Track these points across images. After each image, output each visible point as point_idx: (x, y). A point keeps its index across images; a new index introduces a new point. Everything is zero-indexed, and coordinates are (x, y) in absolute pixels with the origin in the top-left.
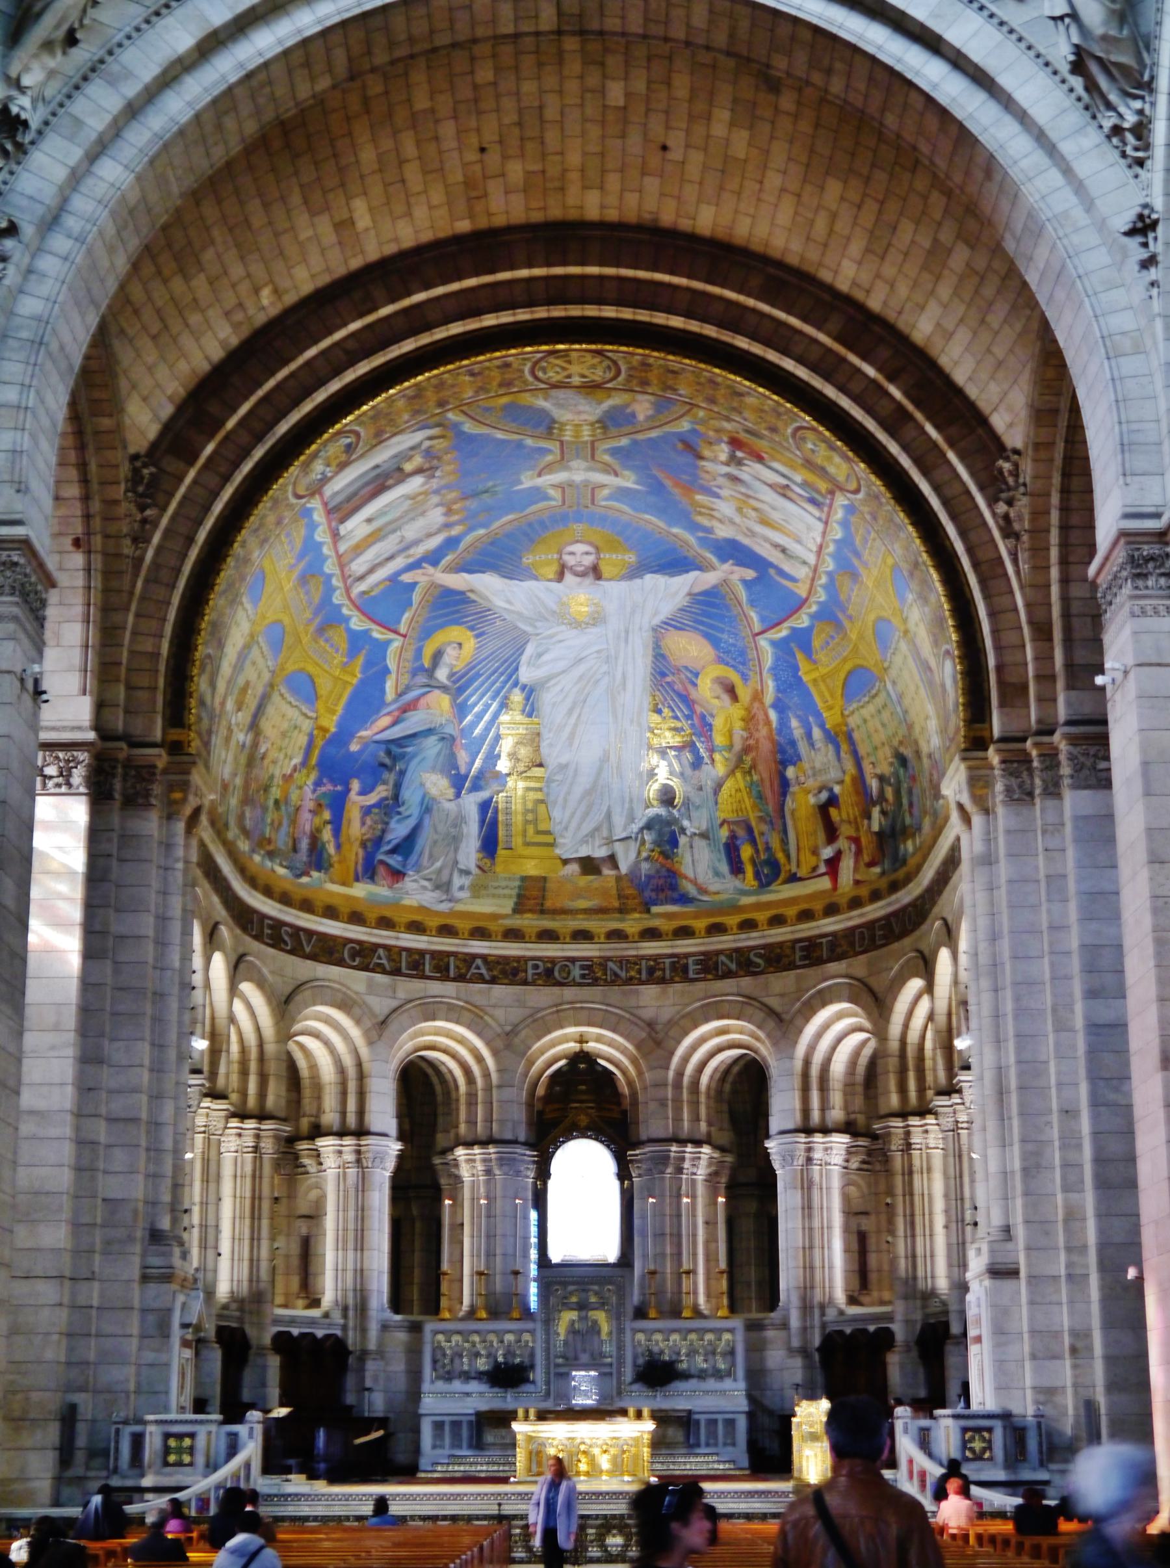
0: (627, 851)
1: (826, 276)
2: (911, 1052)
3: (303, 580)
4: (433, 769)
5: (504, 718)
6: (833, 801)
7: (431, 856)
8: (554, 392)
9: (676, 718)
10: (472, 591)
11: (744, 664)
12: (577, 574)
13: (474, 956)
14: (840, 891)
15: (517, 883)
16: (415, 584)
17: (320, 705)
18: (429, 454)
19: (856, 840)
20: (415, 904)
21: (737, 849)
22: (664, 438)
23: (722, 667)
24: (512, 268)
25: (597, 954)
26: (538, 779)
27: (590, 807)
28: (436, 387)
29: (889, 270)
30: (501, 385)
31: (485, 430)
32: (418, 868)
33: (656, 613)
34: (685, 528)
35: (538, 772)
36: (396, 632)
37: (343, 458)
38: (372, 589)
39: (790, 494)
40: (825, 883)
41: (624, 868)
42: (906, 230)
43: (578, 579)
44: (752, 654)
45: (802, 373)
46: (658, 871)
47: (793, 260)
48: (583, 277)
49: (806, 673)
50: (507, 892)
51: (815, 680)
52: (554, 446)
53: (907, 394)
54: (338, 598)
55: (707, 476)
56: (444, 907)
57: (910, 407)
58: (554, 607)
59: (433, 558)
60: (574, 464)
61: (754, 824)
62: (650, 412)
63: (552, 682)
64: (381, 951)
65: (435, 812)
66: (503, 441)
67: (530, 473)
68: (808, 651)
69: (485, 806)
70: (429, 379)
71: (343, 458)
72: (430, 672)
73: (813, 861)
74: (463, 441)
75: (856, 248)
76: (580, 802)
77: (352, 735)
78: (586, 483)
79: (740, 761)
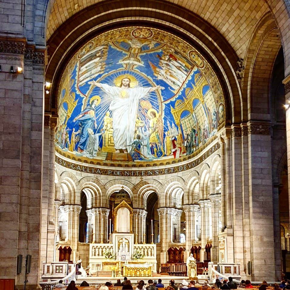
0: (129, 148)
1: (202, 16)
2: (191, 192)
3: (71, 80)
5: (105, 118)
6: (175, 139)
9: (142, 120)
10: (102, 88)
11: (158, 109)
12: (124, 86)
14: (176, 158)
16: (91, 84)
17: (68, 110)
18: (102, 52)
19: (181, 148)
21: (153, 149)
22: (154, 54)
24: (132, 7)
27: (122, 138)
29: (218, 15)
30: (125, 36)
31: (115, 48)
33: (140, 96)
34: (151, 77)
36: (85, 95)
38: (82, 84)
39: (181, 69)
40: (173, 157)
41: (129, 152)
42: (225, 5)
44: (160, 107)
47: (195, 11)
48: (147, 11)
49: (172, 111)
51: (174, 113)
53: (218, 45)
54: (76, 86)
55: (161, 64)
57: (218, 48)
59: (95, 79)
60: (131, 59)
61: (157, 144)
65: (90, 137)
67: (121, 60)
68: (174, 107)
69: (100, 137)
70: (111, 32)
73: (170, 152)
74: (111, 50)
75: (211, 9)
76: (120, 136)
77: (74, 118)
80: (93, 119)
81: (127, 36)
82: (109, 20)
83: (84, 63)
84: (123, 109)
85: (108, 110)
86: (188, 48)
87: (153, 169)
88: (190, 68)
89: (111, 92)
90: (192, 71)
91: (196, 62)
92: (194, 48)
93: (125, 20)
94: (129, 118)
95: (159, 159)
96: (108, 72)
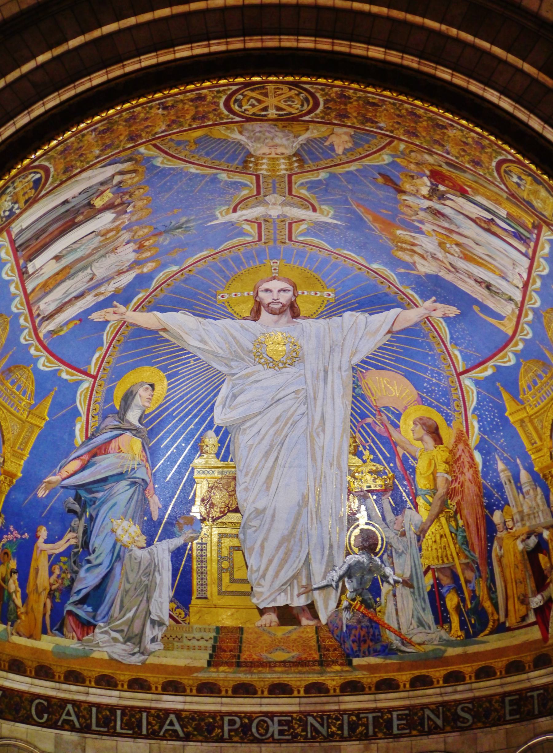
4: (125, 515)
5: (198, 461)
7: (122, 607)
8: (248, 125)
9: (376, 460)
10: (164, 330)
11: (448, 405)
12: (273, 312)
13: (167, 712)
15: (213, 634)
16: (107, 322)
20: (106, 657)
21: (443, 598)
23: (424, 407)
25: (296, 708)
26: (233, 525)
27: (287, 554)
28: (126, 121)
30: (194, 119)
31: (179, 164)
32: (108, 618)
34: (385, 264)
35: (233, 517)
37: (32, 194)
38: (61, 328)
39: (494, 229)
40: (535, 633)
41: (324, 620)
43: (275, 317)
45: (506, 104)
46: (359, 622)
50: (202, 643)
51: (522, 421)
52: (249, 180)
54: (25, 338)
55: (408, 211)
56: (136, 660)
58: (251, 347)
60: (270, 198)
61: (459, 571)
62: (350, 145)
63: (248, 424)
64: (69, 707)
65: (126, 560)
66: (197, 175)
67: (225, 208)
71: (32, 194)
72: (121, 414)
73: (522, 610)
76: (278, 547)
77: (40, 481)
78: (283, 218)
79: (444, 505)
80: (138, 475)
81: (204, 117)
82: (104, 65)
83: (35, 244)
84: (278, 419)
85: (210, 426)
86: (483, 147)
87: (446, 698)
88: (530, 226)
89: (212, 346)
90: (542, 239)
91: (534, 203)
92: (507, 147)
93: (179, 55)
94: (314, 459)
95: (472, 649)
96: (175, 262)
